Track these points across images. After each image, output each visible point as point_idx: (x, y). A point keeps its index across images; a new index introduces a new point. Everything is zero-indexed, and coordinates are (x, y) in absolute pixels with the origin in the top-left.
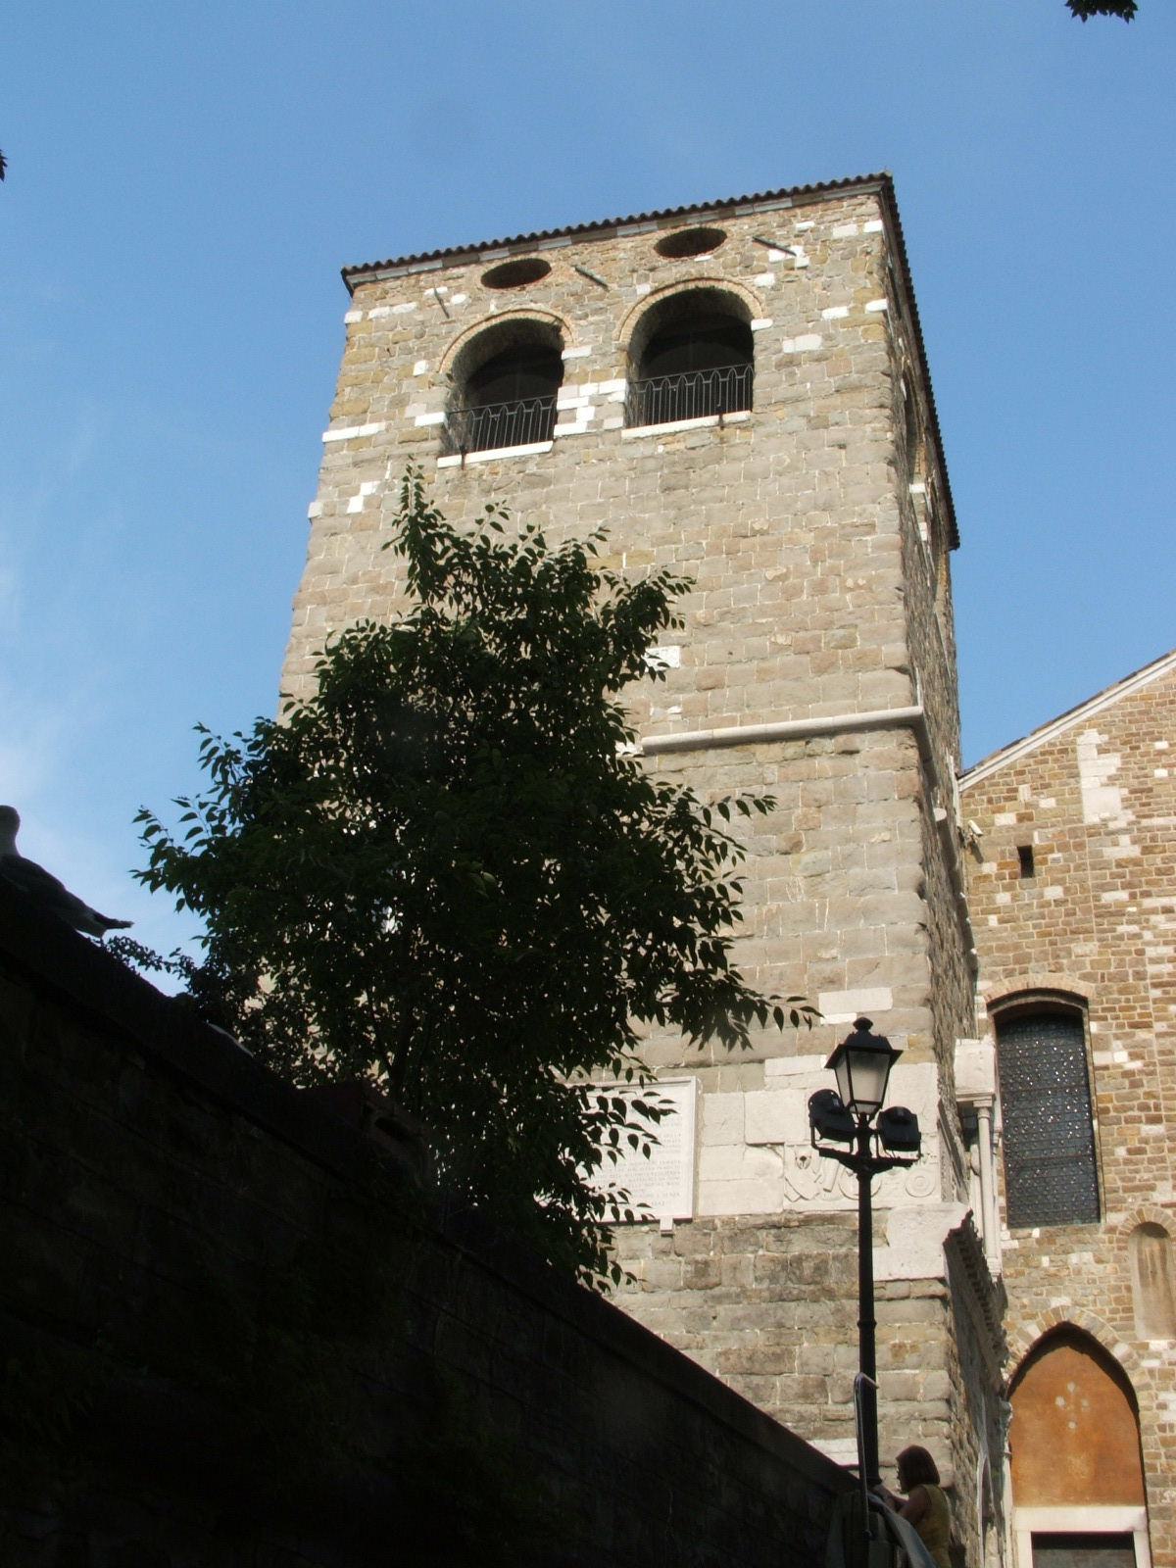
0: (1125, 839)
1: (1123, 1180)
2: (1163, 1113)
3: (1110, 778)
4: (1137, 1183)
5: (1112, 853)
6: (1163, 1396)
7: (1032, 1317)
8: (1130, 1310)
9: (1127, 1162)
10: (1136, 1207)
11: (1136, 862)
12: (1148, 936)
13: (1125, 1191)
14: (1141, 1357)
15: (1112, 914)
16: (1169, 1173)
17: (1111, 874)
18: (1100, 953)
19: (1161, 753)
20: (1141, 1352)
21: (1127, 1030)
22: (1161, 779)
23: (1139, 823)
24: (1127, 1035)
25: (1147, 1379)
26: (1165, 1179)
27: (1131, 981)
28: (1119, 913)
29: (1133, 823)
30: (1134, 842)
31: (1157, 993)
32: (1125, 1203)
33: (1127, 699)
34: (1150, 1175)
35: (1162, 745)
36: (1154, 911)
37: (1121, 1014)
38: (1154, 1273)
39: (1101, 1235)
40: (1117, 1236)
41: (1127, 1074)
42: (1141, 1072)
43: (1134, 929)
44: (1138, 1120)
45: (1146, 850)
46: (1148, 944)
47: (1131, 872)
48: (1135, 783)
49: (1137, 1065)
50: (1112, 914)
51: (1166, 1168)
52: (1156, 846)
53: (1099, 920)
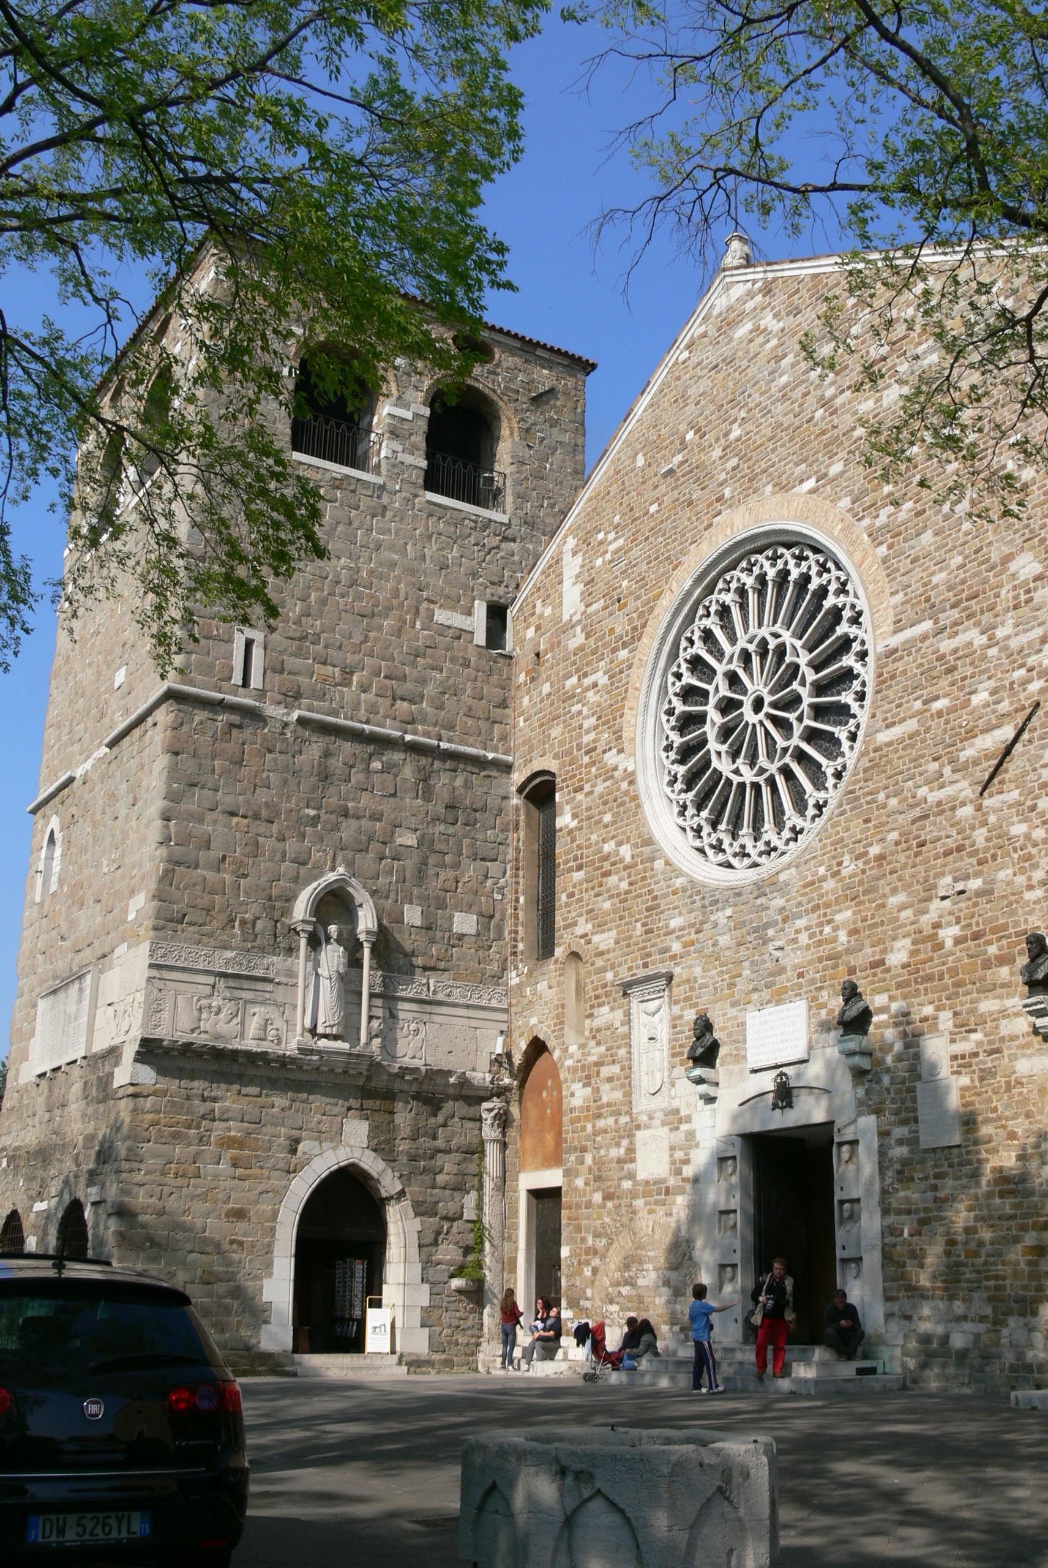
0: (578, 629)
7: (522, 1035)
8: (562, 1023)
9: (567, 905)
12: (585, 712)
15: (569, 698)
19: (601, 543)
31: (586, 759)
33: (590, 500)
39: (552, 967)
41: (570, 832)
43: (576, 708)
44: (570, 870)
45: (588, 636)
46: (586, 718)
48: (586, 577)
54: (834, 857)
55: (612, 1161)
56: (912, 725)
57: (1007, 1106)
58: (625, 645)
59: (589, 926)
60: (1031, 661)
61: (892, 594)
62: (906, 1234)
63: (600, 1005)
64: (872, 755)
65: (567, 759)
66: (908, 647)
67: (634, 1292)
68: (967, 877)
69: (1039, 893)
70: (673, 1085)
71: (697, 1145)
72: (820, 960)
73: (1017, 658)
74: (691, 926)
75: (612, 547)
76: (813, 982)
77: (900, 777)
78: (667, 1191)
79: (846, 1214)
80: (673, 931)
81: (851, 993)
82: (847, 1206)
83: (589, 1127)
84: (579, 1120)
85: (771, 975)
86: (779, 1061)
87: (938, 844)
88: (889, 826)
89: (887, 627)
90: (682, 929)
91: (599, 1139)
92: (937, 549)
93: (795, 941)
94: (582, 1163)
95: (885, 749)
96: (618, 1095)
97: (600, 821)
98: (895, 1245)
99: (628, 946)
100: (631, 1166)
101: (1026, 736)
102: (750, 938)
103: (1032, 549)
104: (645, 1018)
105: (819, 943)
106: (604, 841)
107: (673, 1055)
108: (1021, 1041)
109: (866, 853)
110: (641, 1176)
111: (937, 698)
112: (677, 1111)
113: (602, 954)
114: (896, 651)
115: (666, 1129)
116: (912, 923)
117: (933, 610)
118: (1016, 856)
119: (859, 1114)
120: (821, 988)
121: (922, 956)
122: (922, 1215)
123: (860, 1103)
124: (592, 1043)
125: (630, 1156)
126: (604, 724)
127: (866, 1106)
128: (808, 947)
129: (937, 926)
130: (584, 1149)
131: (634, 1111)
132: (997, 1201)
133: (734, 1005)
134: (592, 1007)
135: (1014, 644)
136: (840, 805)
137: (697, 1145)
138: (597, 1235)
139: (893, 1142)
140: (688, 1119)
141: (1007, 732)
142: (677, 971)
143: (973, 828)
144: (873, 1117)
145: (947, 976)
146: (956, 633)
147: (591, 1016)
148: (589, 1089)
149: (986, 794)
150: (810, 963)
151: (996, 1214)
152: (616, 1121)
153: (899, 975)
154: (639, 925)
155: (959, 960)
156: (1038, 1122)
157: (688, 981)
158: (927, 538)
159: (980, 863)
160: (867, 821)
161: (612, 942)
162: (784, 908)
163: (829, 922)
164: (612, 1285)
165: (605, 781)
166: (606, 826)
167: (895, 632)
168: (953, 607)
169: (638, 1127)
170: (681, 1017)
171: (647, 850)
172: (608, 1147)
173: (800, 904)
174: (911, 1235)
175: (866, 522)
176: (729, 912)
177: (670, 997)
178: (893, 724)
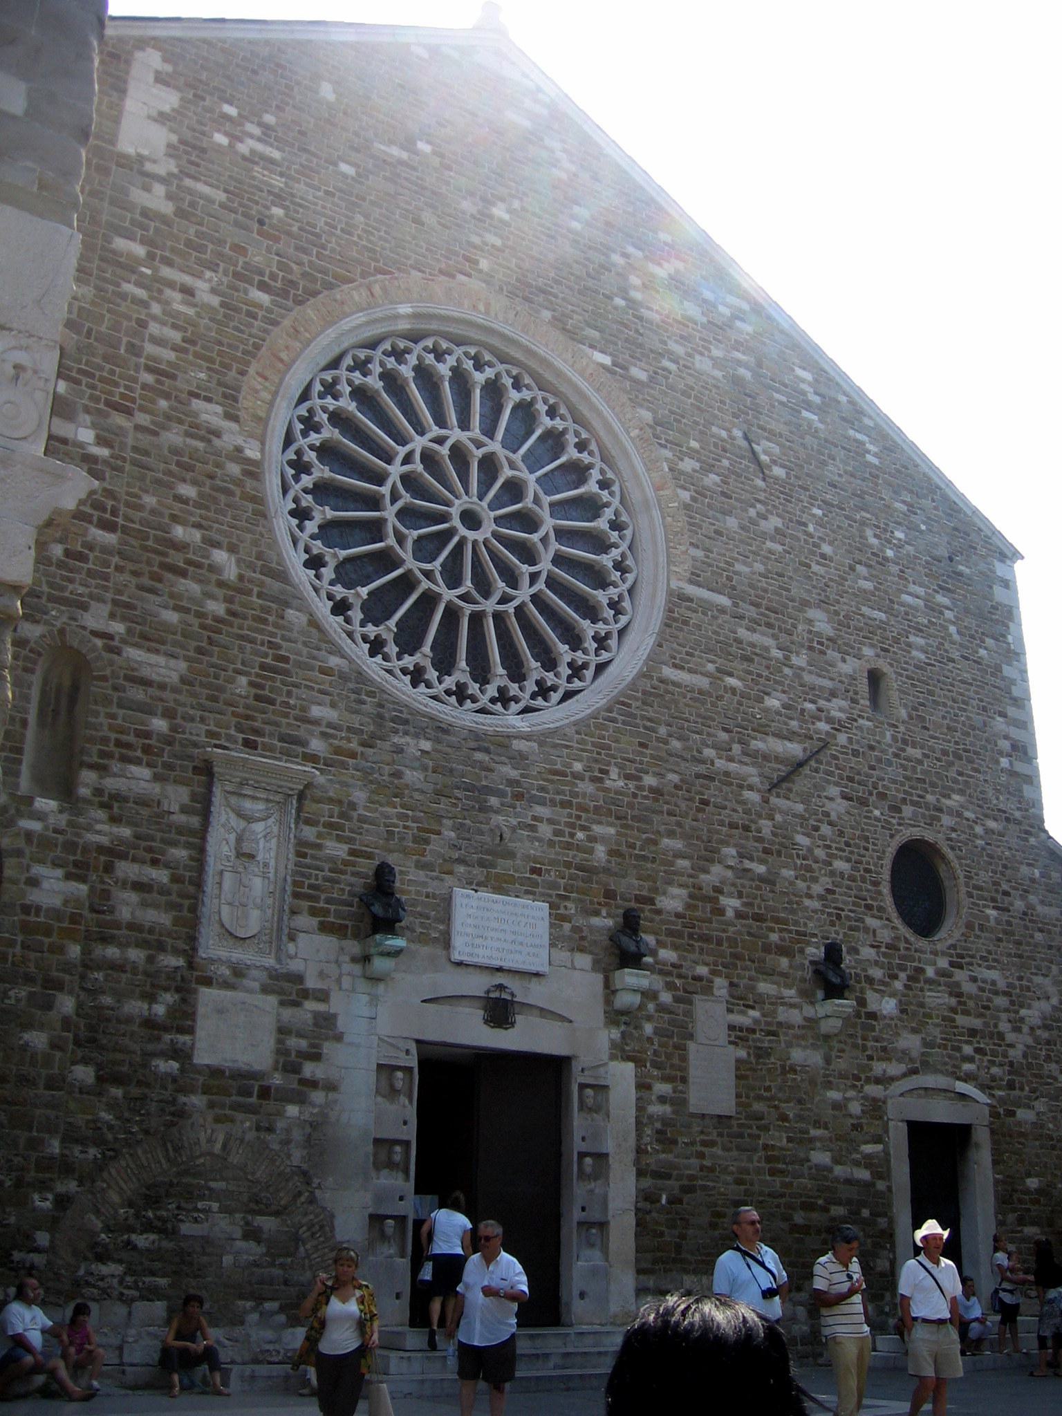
0: (159, 189)
1: (51, 585)
2: (120, 521)
3: (161, 114)
4: (67, 594)
5: (139, 197)
6: (38, 870)
8: (19, 751)
9: (61, 565)
10: (58, 624)
11: (164, 219)
12: (156, 309)
13: (49, 600)
14: (20, 814)
15: (119, 265)
16: (109, 596)
17: (132, 219)
18: (93, 303)
20: (22, 808)
21: (101, 406)
22: (220, 145)
23: (181, 180)
24: (99, 411)
25: (21, 843)
26: (100, 600)
27: (122, 351)
28: (128, 266)
29: (170, 174)
30: (169, 197)
31: (149, 378)
32: (46, 613)
34: (87, 591)
35: (231, 111)
36: (171, 284)
37: (100, 385)
38: (56, 712)
40: (24, 652)
42: (105, 462)
45: (180, 213)
47: (156, 229)
48: (188, 135)
49: (104, 452)
50: (119, 265)
51: (106, 588)
52: (194, 215)
53: (104, 265)
54: (596, 761)
55: (129, 1020)
56: (703, 682)
57: (780, 1089)
58: (263, 287)
59: (118, 628)
60: (822, 703)
61: (692, 544)
62: (664, 1201)
63: (125, 759)
64: (655, 682)
65: (101, 349)
66: (705, 607)
67: (167, 1245)
68: (751, 859)
69: (816, 904)
70: (292, 938)
71: (339, 1038)
72: (568, 865)
73: (812, 693)
74: (359, 732)
75: (251, 143)
76: (554, 886)
77: (686, 724)
78: (265, 1093)
79: (588, 1170)
80: (316, 722)
81: (630, 923)
82: (588, 1160)
83: (75, 951)
84: (48, 932)
85: (488, 852)
86: (506, 965)
87: (723, 812)
88: (669, 767)
89: (683, 569)
90: (330, 725)
91: (99, 976)
92: (741, 541)
93: (532, 828)
94: (48, 1006)
95: (671, 688)
96: (164, 919)
97: (171, 487)
98: (650, 1212)
99: (214, 699)
100: (184, 1039)
101: (813, 763)
102: (457, 793)
103: (828, 611)
104: (234, 821)
105: (568, 846)
106: (175, 519)
107: (296, 895)
108: (797, 1031)
109: (639, 779)
110: (203, 1057)
111: (731, 675)
112: (298, 978)
113: (146, 683)
114: (690, 600)
115: (273, 1000)
116: (691, 876)
117: (731, 590)
118: (799, 862)
119: (613, 1057)
120: (566, 898)
121: (698, 914)
122: (685, 1182)
123: (613, 1045)
124: (101, 814)
125: (183, 1019)
126: (197, 355)
127: (621, 1052)
128: (551, 843)
129: (719, 891)
130: (59, 986)
131: (202, 953)
132: (768, 1178)
133: (421, 866)
134: (109, 755)
135: (808, 678)
136: (610, 710)
137: (339, 1038)
138: (71, 1137)
139: (654, 1098)
140: (323, 996)
141: (795, 749)
142: (320, 779)
143: (760, 816)
144: (631, 1065)
145: (725, 944)
146: (754, 631)
147: (102, 769)
148: (83, 888)
149: (774, 791)
150: (552, 862)
151: (767, 1190)
152: (150, 959)
153: (673, 923)
154: (243, 680)
155: (739, 933)
156: (809, 1109)
157: (340, 802)
158: (732, 523)
159: (766, 851)
160: (641, 745)
161: (174, 678)
162: (517, 783)
163: (583, 828)
164: (108, 1229)
165: (188, 434)
166: (179, 498)
167: (691, 582)
168: (752, 604)
169: (208, 982)
170: (319, 847)
171: (274, 586)
172: (120, 996)
173: (542, 789)
174: (669, 1202)
175: (667, 453)
176: (426, 745)
177: (299, 810)
178: (682, 668)
